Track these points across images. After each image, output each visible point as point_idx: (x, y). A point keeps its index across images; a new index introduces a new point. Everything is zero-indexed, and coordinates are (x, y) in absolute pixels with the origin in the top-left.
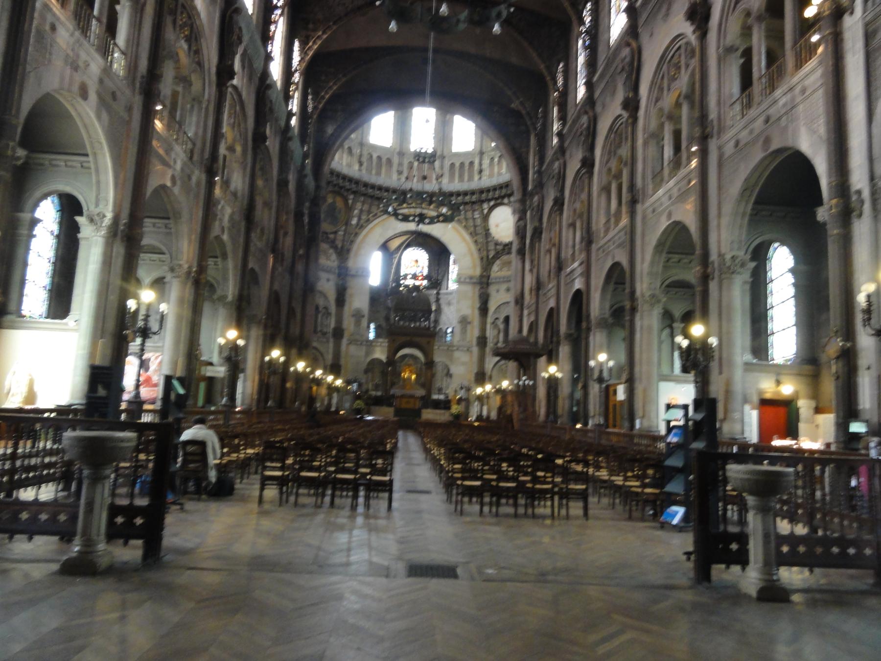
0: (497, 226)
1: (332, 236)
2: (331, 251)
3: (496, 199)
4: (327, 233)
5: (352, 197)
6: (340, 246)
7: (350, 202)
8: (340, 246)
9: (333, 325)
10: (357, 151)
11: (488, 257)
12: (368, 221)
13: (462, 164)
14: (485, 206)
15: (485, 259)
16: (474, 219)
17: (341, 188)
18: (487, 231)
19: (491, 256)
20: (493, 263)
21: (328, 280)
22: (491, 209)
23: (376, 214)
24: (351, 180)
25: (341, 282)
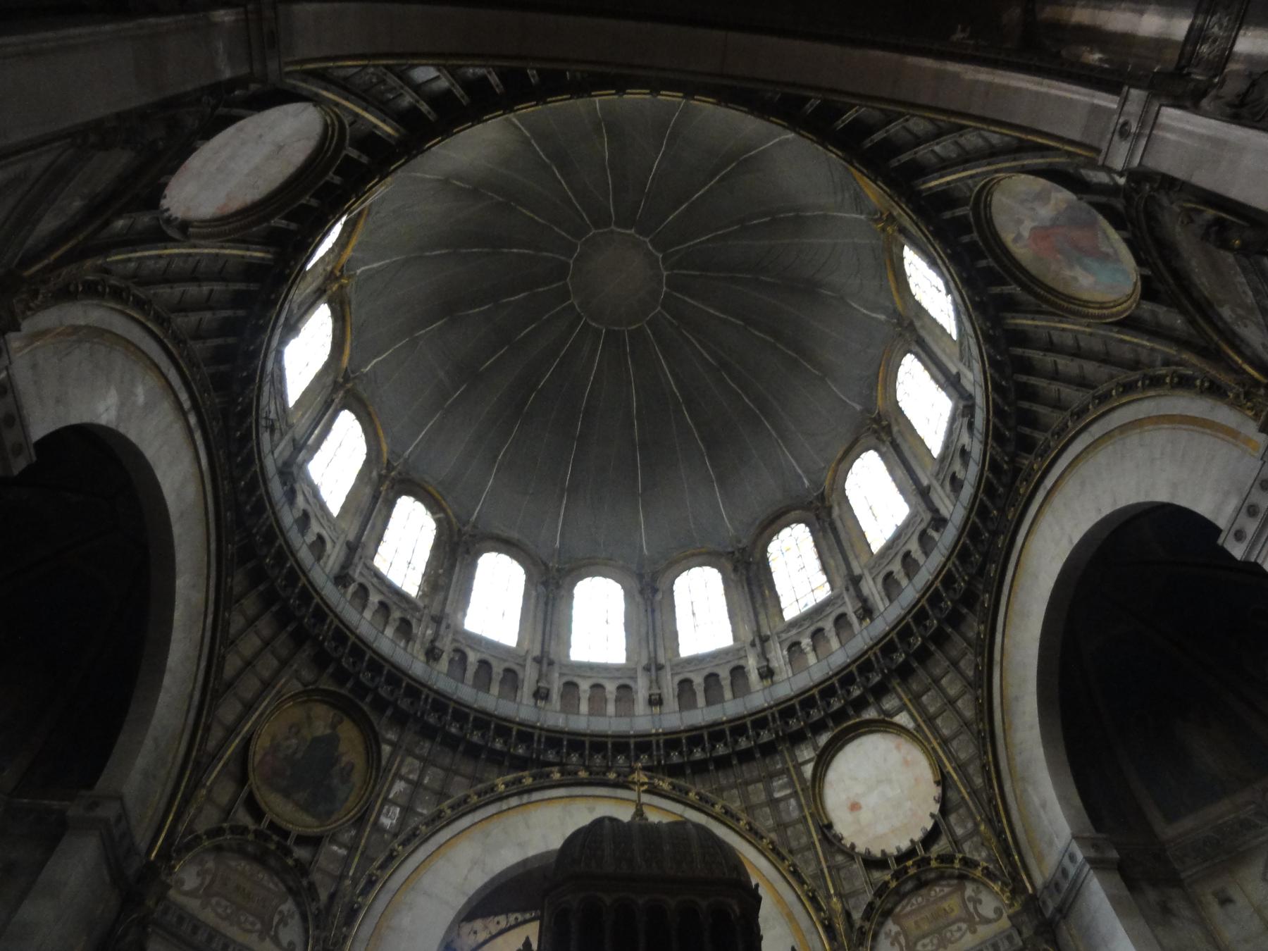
0: (855, 807)
1: (301, 853)
2: (288, 906)
3: (840, 716)
4: (285, 834)
5: (391, 736)
6: (324, 896)
7: (386, 749)
8: (324, 896)
10: (424, 631)
11: (848, 915)
12: (437, 822)
13: (712, 679)
14: (806, 753)
15: (840, 926)
16: (773, 803)
17: (361, 690)
18: (826, 828)
19: (857, 916)
20: (875, 937)
22: (824, 760)
23: (465, 800)
24: (396, 676)
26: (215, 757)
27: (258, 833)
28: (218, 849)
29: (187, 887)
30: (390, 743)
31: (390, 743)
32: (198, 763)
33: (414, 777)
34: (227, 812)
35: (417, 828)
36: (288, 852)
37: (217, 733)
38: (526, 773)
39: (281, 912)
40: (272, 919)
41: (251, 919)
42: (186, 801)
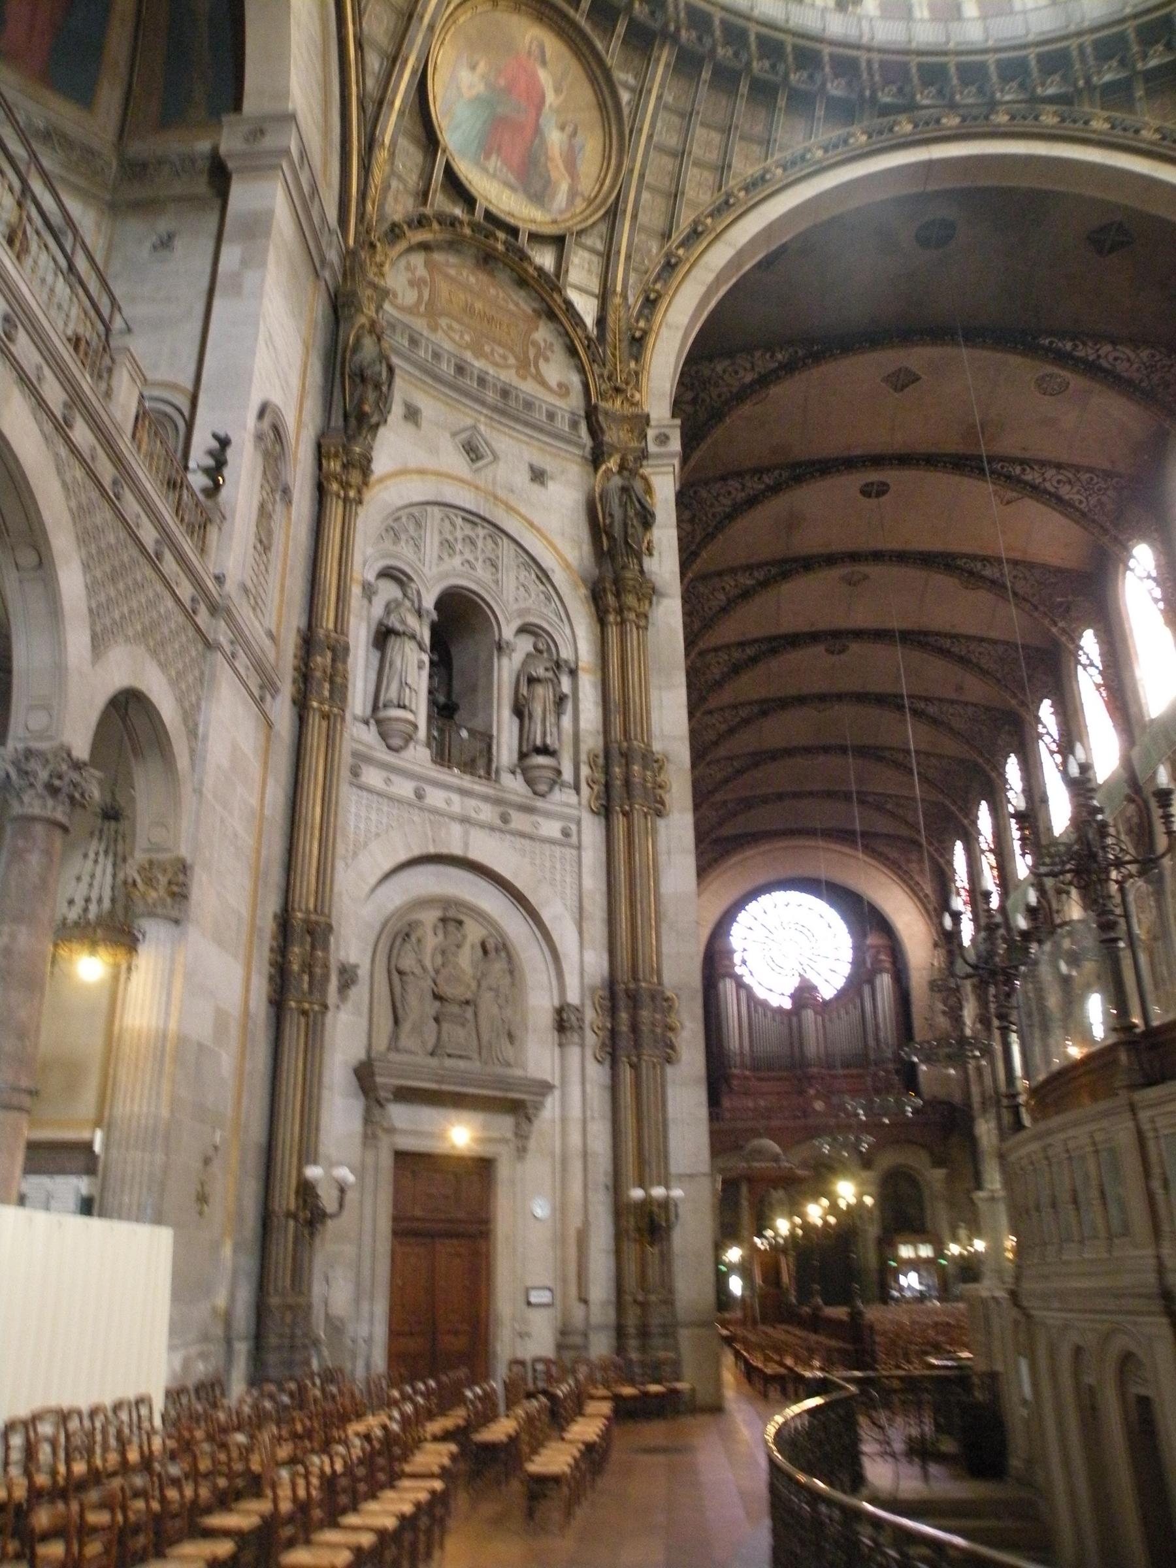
4: (514, 231)
6: (589, 320)
7: (625, 96)
9: (592, 742)
21: (538, 476)
25: (617, 481)
26: (381, 102)
27: (474, 226)
28: (425, 247)
29: (399, 301)
30: (626, 86)
31: (626, 86)
32: (362, 107)
33: (673, 141)
34: (423, 196)
35: (696, 223)
36: (524, 257)
37: (374, 62)
38: (852, 129)
39: (535, 344)
40: (526, 353)
41: (501, 351)
42: (366, 169)
